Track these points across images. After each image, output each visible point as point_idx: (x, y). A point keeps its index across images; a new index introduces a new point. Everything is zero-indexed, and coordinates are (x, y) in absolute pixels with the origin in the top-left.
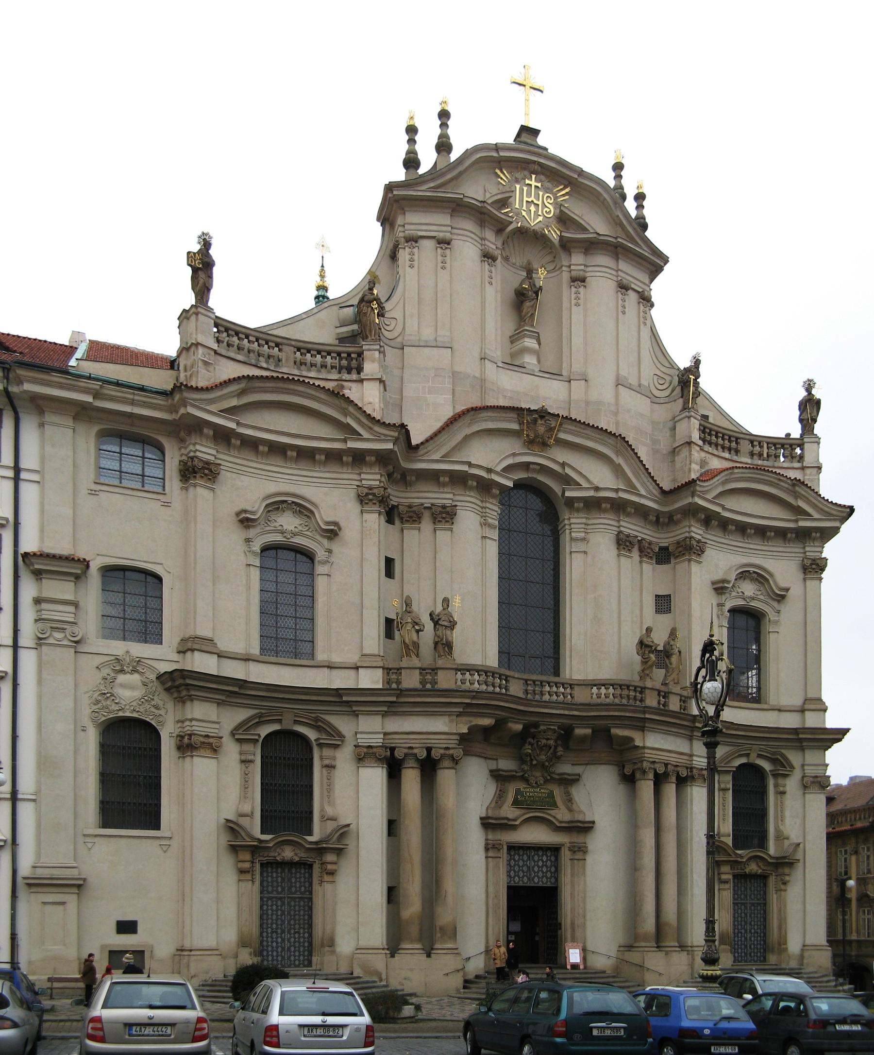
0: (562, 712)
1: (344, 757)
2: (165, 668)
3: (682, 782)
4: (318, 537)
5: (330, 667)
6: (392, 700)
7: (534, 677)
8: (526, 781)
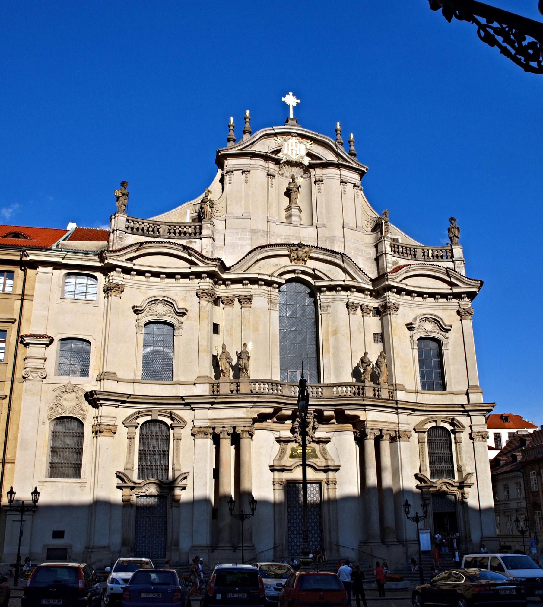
1: (186, 432)
2: (88, 390)
3: (393, 440)
6: (214, 400)
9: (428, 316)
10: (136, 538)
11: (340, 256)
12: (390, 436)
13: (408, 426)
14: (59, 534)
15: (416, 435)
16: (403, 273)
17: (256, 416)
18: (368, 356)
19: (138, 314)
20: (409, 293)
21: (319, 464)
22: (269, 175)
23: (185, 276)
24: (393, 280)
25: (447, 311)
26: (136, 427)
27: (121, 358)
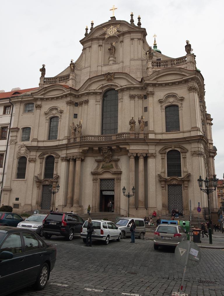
0: (106, 143)
5: (59, 140)
7: (106, 135)
8: (105, 161)
9: (171, 94)
10: (42, 201)
11: (124, 74)
12: (143, 156)
13: (155, 151)
14: (17, 199)
15: (160, 155)
16: (155, 76)
17: (81, 151)
18: (134, 119)
20: (161, 85)
21: (114, 171)
22: (99, 46)
23: (62, 97)
25: (181, 91)
26: (43, 159)
27: (40, 134)
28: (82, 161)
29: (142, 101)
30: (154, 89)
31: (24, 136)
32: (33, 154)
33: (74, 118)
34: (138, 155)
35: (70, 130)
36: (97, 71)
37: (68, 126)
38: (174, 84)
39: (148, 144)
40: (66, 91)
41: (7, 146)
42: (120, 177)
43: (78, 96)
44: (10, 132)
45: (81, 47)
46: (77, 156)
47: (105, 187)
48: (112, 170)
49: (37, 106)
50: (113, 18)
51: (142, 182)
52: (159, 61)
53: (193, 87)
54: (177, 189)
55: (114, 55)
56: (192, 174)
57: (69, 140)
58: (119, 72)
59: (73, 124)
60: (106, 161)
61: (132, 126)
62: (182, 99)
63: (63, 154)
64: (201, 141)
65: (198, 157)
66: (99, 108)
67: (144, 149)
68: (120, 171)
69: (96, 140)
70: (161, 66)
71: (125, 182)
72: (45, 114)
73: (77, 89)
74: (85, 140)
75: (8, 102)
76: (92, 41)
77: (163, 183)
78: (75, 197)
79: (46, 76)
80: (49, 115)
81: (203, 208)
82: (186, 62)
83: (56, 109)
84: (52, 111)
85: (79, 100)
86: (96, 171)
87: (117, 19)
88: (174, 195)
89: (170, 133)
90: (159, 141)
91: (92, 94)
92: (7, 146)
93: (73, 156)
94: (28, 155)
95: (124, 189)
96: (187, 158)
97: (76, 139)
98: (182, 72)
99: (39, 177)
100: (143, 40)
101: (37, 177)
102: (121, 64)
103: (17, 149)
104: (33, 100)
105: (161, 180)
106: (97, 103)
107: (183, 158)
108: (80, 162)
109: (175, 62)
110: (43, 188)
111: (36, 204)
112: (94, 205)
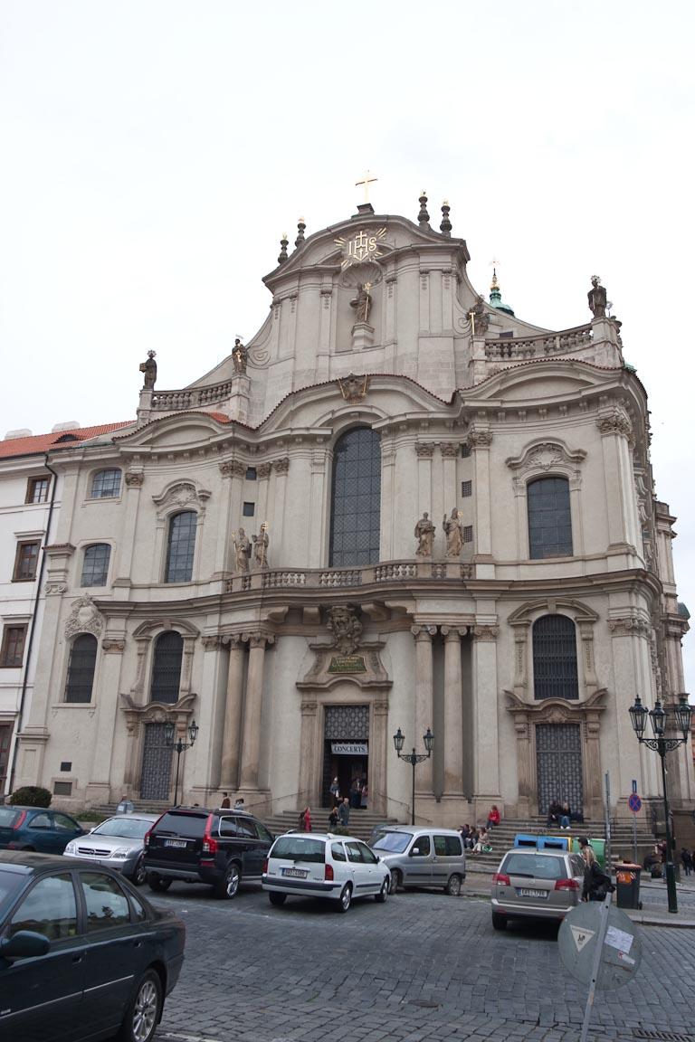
0: (342, 594)
4: (199, 502)
5: (197, 584)
7: (342, 569)
8: (339, 650)
9: (545, 442)
11: (399, 381)
12: (459, 635)
13: (495, 617)
15: (511, 632)
17: (266, 618)
18: (429, 518)
19: (159, 505)
20: (513, 413)
21: (368, 680)
22: (323, 293)
23: (207, 450)
24: (475, 398)
25: (577, 433)
27: (139, 563)
28: (269, 647)
29: (454, 462)
30: (492, 426)
31: (90, 570)
32: (117, 627)
33: (244, 515)
34: (444, 631)
35: (231, 551)
36: (316, 370)
37: (226, 542)
38: (553, 409)
39: (474, 595)
40: (219, 432)
41: (37, 600)
42: (387, 700)
43: (258, 448)
44: (48, 558)
45: (268, 297)
46: (251, 633)
47: (340, 729)
48: (360, 677)
49: (129, 477)
50: (366, 208)
51: (454, 717)
52: (507, 341)
53: (614, 419)
54: (565, 738)
55: (367, 321)
56: (610, 690)
57: (228, 582)
58: (385, 373)
59: (242, 533)
60: (343, 651)
61: (425, 541)
62: (579, 457)
63: (209, 625)
64: (639, 586)
65: (630, 638)
66: (321, 484)
67: (461, 612)
68: (387, 682)
69: (313, 582)
70: (513, 354)
71: (404, 712)
72: (156, 502)
73: (254, 424)
74: (278, 585)
75: (43, 464)
76: (300, 280)
77: (521, 718)
78: (247, 762)
79: (158, 387)
80: (166, 505)
81: (649, 799)
82: (592, 343)
83: (190, 487)
84: (175, 495)
85: (257, 460)
86: (312, 679)
87: (379, 210)
88: (557, 758)
89: (543, 561)
90: (507, 588)
91: (301, 440)
92: (37, 600)
93: (241, 635)
94: (100, 628)
95: (399, 737)
96: (596, 642)
97: (250, 579)
98: (579, 372)
99: (133, 700)
100: (458, 276)
101: (127, 699)
102: (390, 350)
103: (68, 611)
104: (116, 458)
105: (514, 708)
106: (315, 469)
107: (584, 640)
108: (262, 651)
109: (557, 343)
110: (147, 731)
111: (125, 782)
112: (304, 787)
